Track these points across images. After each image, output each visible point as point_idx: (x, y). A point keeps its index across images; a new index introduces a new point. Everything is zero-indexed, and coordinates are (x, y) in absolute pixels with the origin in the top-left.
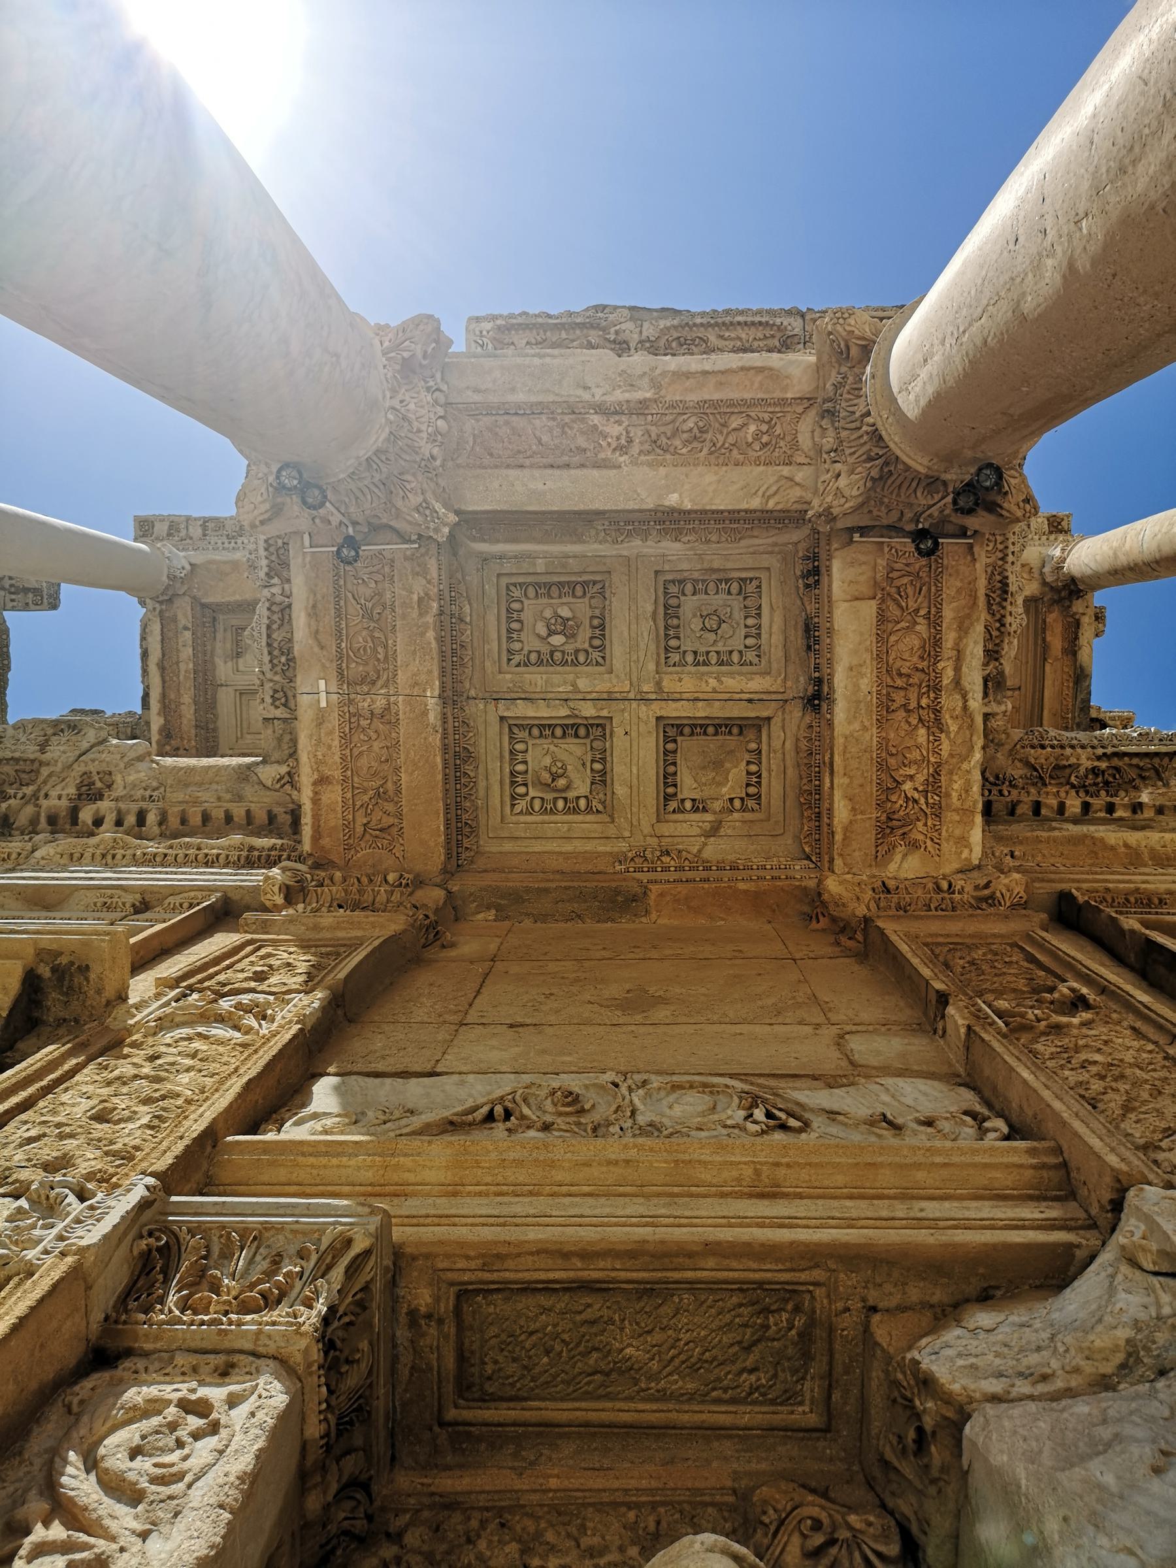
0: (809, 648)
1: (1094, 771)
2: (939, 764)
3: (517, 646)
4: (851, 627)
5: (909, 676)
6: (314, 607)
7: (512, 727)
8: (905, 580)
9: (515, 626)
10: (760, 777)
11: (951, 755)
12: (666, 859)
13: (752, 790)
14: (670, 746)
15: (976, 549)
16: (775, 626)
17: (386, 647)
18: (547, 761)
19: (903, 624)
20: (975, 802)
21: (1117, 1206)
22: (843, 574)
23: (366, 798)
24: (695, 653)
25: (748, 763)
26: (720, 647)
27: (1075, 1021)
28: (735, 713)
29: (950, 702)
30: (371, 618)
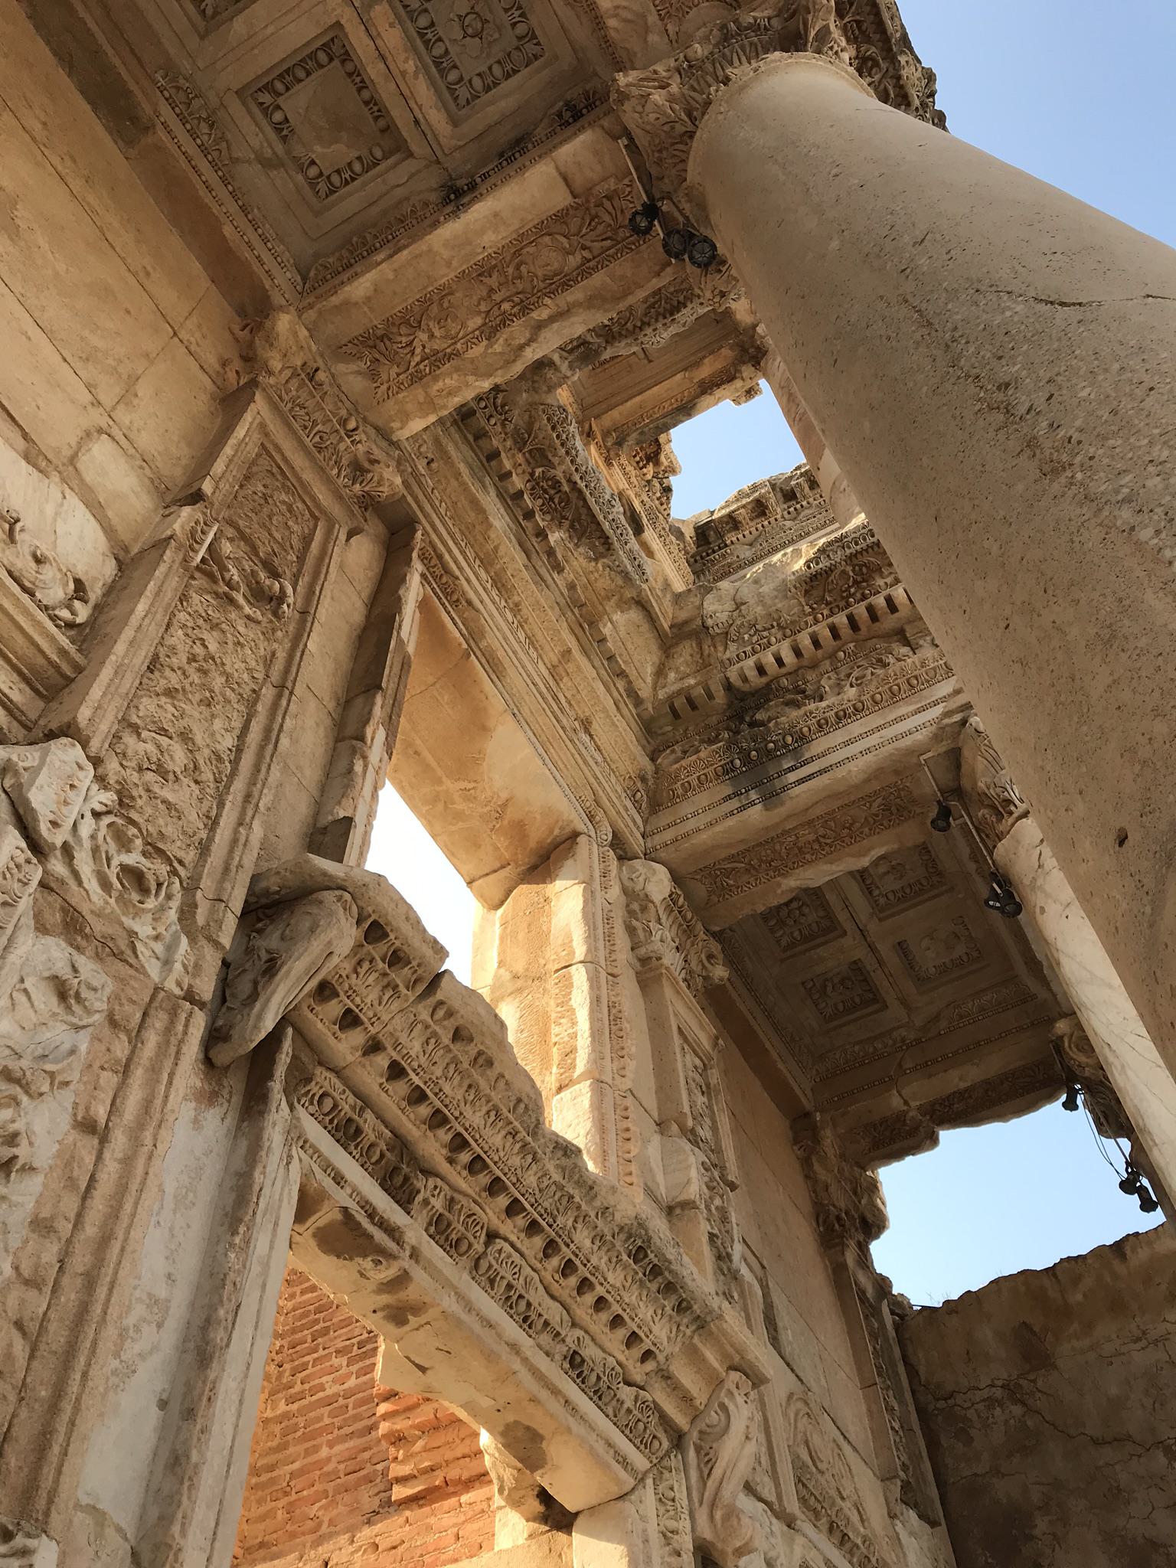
0: (501, 155)
1: (556, 484)
2: (458, 354)
5: (521, 278)
8: (607, 218)
10: (353, 179)
11: (472, 360)
12: (204, 128)
13: (336, 179)
14: (322, 57)
15: (669, 270)
20: (445, 407)
21: (51, 736)
22: (578, 149)
24: (432, 24)
25: (359, 158)
27: (247, 610)
28: (395, 113)
29: (518, 330)
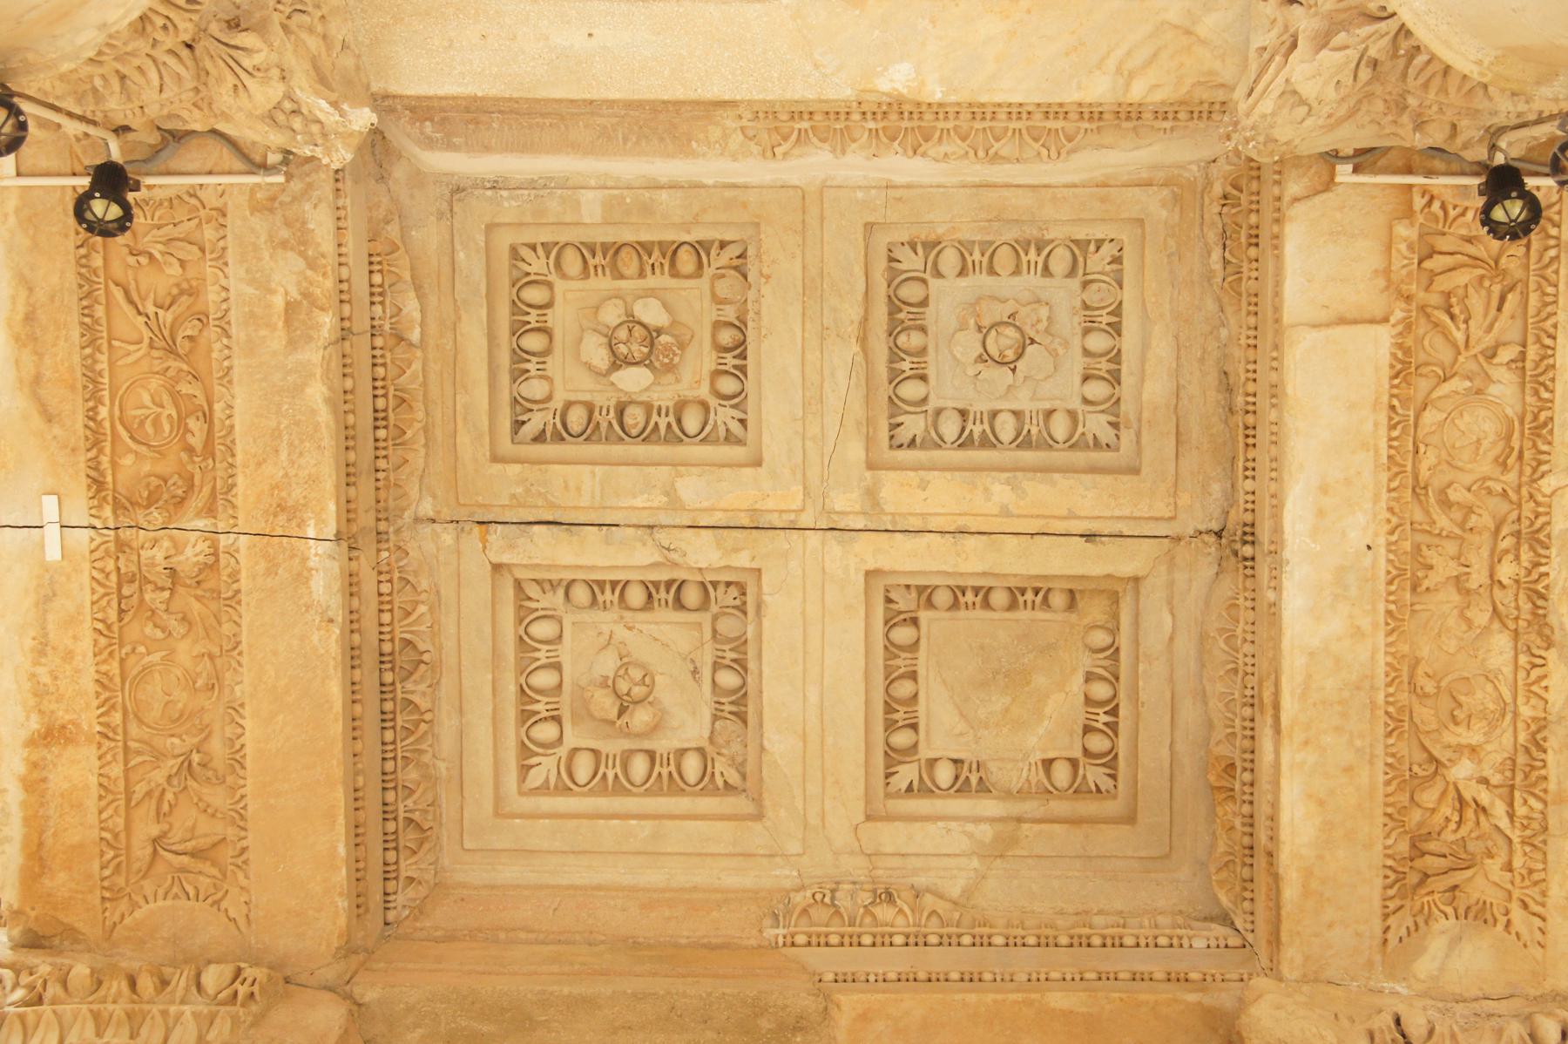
2: (1542, 724)
3: (535, 389)
4: (1330, 391)
5: (1470, 510)
6: (29, 318)
7: (525, 594)
8: (1462, 278)
9: (533, 342)
10: (1114, 712)
12: (884, 912)
14: (903, 635)
16: (1156, 369)
17: (208, 418)
18: (607, 664)
19: (1457, 384)
23: (159, 776)
24: (963, 413)
26: (1023, 402)
30: (171, 351)
